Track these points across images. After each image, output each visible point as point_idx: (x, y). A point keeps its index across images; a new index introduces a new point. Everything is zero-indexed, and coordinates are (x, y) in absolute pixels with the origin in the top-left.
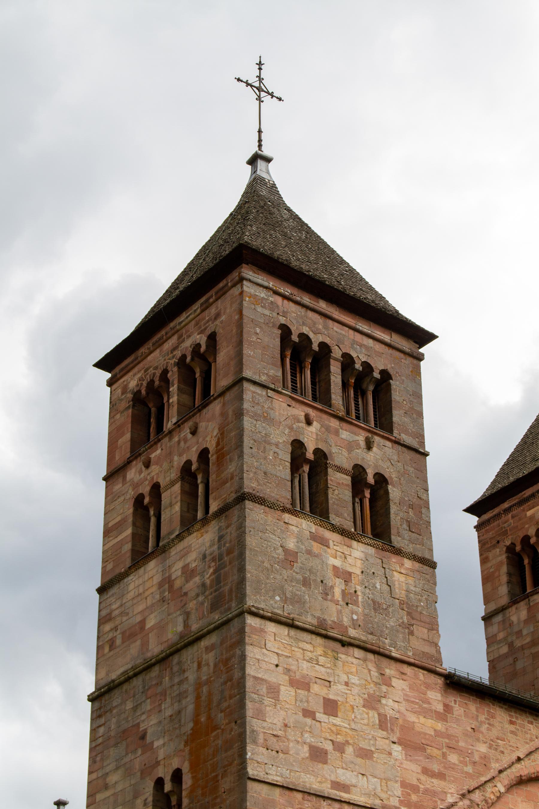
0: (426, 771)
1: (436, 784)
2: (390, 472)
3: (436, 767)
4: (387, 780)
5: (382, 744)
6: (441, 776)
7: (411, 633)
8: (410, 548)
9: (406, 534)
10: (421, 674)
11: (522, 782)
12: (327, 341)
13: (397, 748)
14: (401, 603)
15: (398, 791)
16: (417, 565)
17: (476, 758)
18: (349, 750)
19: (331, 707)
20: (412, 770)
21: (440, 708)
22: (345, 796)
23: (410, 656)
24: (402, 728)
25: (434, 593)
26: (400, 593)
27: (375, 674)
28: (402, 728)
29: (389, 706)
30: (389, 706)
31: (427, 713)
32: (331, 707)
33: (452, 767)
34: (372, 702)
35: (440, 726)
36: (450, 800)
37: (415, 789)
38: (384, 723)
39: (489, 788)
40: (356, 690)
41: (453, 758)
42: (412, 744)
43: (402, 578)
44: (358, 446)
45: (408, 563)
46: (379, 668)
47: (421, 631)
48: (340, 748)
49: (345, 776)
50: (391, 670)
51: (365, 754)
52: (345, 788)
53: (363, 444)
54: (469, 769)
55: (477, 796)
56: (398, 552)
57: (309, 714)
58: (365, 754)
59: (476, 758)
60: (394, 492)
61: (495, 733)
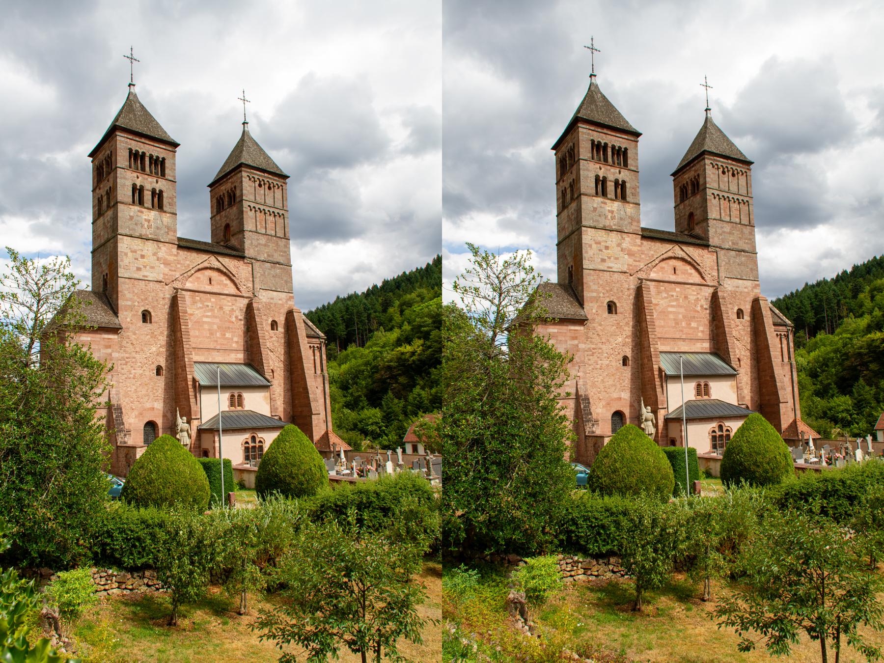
2: (163, 189)
8: (169, 211)
11: (199, 270)
15: (162, 276)
19: (143, 257)
30: (160, 255)
32: (143, 257)
42: (166, 263)
50: (161, 245)
56: (165, 212)
57: (136, 259)
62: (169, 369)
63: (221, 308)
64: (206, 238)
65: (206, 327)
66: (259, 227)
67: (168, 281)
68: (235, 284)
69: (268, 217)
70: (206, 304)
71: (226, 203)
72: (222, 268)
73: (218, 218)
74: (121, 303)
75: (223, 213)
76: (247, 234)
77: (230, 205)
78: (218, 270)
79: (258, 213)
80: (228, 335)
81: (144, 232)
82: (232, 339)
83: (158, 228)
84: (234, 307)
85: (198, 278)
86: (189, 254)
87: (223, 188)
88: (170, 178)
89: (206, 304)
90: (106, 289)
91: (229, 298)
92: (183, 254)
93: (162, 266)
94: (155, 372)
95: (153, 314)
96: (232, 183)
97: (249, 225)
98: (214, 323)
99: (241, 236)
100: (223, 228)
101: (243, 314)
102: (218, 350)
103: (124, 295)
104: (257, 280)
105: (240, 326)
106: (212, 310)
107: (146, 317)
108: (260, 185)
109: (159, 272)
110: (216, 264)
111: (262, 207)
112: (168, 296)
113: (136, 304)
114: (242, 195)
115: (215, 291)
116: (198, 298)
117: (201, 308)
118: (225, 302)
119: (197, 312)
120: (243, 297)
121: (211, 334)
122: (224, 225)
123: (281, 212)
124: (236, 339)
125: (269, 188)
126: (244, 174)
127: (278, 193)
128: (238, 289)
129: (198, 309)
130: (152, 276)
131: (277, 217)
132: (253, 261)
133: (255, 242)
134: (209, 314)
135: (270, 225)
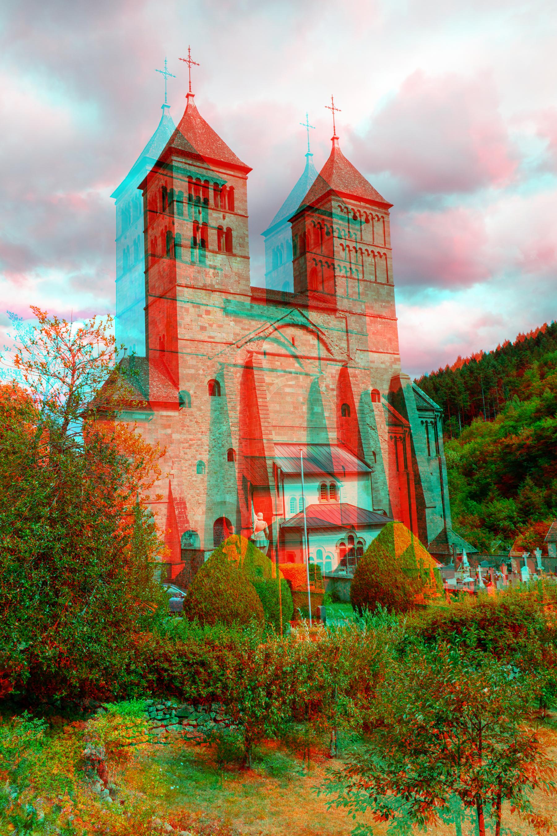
0: (242, 329)
1: (247, 332)
2: (232, 226)
3: (246, 327)
4: (228, 333)
5: (226, 322)
6: (248, 329)
7: (239, 283)
9: (238, 248)
14: (236, 273)
18: (214, 325)
21: (249, 307)
22: (212, 340)
23: (238, 291)
25: (249, 268)
26: (235, 270)
33: (253, 326)
36: (251, 337)
37: (238, 335)
39: (266, 331)
43: (236, 265)
44: (220, 218)
45: (239, 259)
47: (243, 282)
48: (211, 325)
49: (212, 334)
51: (220, 326)
52: (213, 338)
53: (222, 217)
56: (235, 255)
58: (220, 326)
60: (234, 233)
61: (269, 313)
65: (289, 399)
67: (240, 344)
68: (325, 345)
69: (365, 258)
76: (340, 281)
78: (303, 327)
81: (208, 281)
83: (226, 276)
86: (266, 307)
88: (240, 212)
94: (226, 456)
95: (221, 384)
99: (331, 283)
101: (336, 382)
103: (185, 361)
104: (352, 340)
107: (214, 388)
108: (355, 218)
110: (301, 320)
113: (201, 372)
116: (278, 363)
117: (282, 376)
120: (335, 360)
121: (295, 408)
123: (382, 251)
126: (334, 204)
127: (378, 227)
128: (329, 350)
129: (278, 377)
130: (220, 336)
131: (378, 258)
134: (293, 383)
135: (368, 269)
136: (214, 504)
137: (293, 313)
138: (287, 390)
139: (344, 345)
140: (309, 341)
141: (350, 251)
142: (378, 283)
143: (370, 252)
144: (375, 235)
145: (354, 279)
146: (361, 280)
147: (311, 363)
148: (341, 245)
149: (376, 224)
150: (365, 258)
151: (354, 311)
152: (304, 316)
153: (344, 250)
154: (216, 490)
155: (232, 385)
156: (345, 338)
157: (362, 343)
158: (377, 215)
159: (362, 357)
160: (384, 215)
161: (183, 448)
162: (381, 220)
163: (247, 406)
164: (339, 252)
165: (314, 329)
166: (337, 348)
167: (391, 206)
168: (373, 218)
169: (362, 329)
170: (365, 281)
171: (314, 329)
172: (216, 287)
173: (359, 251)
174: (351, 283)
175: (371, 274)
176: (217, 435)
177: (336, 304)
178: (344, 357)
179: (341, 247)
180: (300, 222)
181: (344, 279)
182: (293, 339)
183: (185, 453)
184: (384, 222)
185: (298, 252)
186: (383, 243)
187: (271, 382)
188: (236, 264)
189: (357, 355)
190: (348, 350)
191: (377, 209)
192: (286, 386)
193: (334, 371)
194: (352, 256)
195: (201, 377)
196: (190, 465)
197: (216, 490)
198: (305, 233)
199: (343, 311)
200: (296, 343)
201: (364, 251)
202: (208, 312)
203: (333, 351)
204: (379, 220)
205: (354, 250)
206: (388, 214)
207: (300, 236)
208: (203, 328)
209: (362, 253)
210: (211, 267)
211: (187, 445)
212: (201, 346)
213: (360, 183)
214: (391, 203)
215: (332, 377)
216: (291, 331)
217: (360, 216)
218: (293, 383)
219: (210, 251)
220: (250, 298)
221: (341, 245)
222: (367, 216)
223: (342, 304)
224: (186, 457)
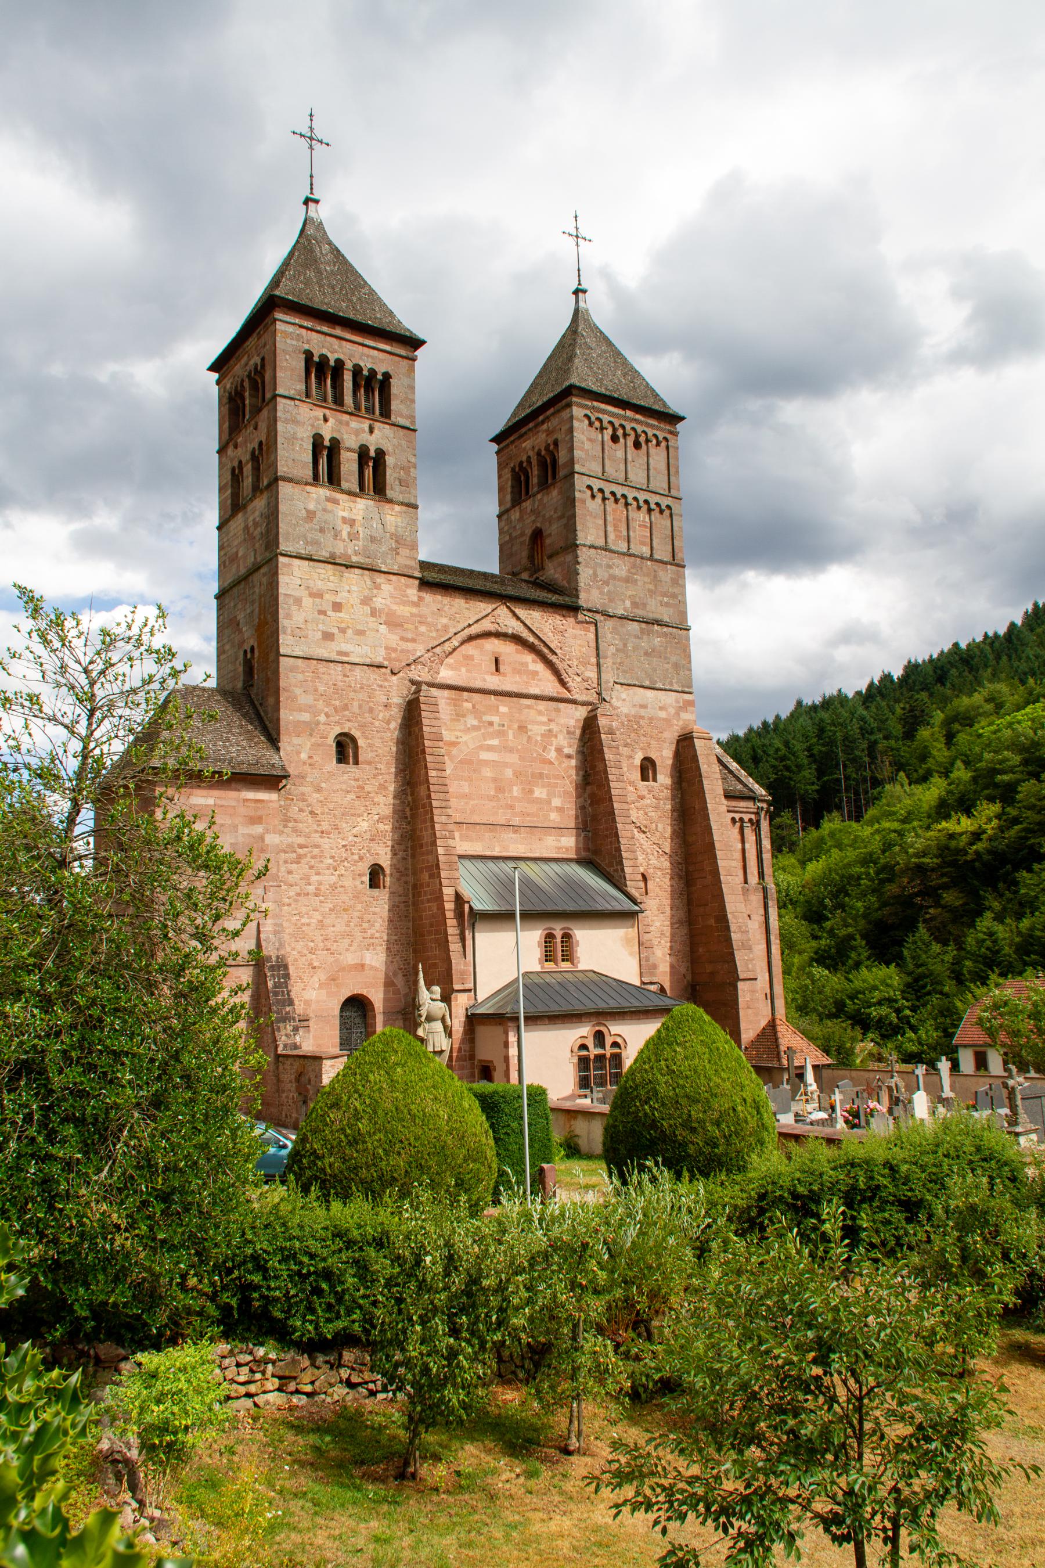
0: (402, 639)
1: (410, 646)
2: (387, 447)
3: (410, 636)
5: (372, 625)
6: (414, 640)
9: (398, 488)
10: (403, 579)
11: (471, 638)
12: (342, 357)
13: (383, 627)
14: (392, 535)
15: (382, 652)
16: (404, 508)
17: (439, 627)
18: (350, 632)
20: (393, 639)
21: (415, 599)
22: (345, 659)
23: (395, 568)
24: (387, 614)
25: (416, 525)
26: (391, 528)
27: (369, 583)
28: (387, 614)
29: (379, 602)
30: (379, 602)
31: (404, 603)
33: (422, 634)
34: (366, 601)
35: (414, 610)
37: (395, 650)
38: (373, 613)
39: (447, 644)
40: (355, 595)
41: (423, 629)
42: (393, 623)
43: (393, 518)
45: (397, 508)
46: (372, 579)
48: (343, 631)
49: (345, 647)
50: (380, 579)
51: (361, 633)
52: (346, 654)
53: (367, 429)
54: (434, 634)
55: (438, 650)
56: (390, 501)
58: (361, 633)
59: (439, 627)
60: (390, 460)
61: (454, 610)
62: (400, 872)
63: (522, 728)
64: (488, 561)
65: (487, 772)
66: (612, 536)
67: (396, 666)
69: (633, 514)
70: (487, 718)
71: (535, 480)
72: (525, 634)
73: (515, 515)
74: (287, 716)
75: (527, 505)
76: (583, 554)
77: (545, 485)
78: (516, 639)
79: (610, 504)
80: (539, 793)
81: (339, 548)
82: (549, 802)
83: (373, 539)
84: (552, 726)
85: (470, 658)
86: (446, 600)
87: (527, 444)
88: (402, 421)
89: (487, 718)
90: (251, 683)
91: (542, 705)
92: (433, 600)
93: (383, 629)
94: (366, 879)
96: (549, 433)
97: (588, 532)
98: (506, 765)
99: (569, 558)
100: (527, 539)
101: (575, 743)
102: (516, 828)
103: (294, 698)
104: (607, 664)
105: (567, 772)
106: (501, 734)
107: (345, 749)
108: (615, 439)
109: (376, 643)
110: (511, 625)
111: (619, 491)
112: (398, 700)
113: (322, 718)
114: (572, 462)
115: (508, 687)
116: (468, 705)
117: (475, 728)
118: (532, 712)
119: (465, 738)
120: (574, 702)
121: (500, 789)
122: (529, 532)
123: (664, 502)
124: (558, 801)
125: (637, 445)
126: (577, 412)
127: (658, 457)
128: (563, 683)
129: (467, 730)
130: (358, 652)
131: (656, 515)
132: (598, 617)
133: (602, 574)
134: (495, 742)
135: (639, 533)
136: (343, 969)
137: (498, 611)
138: (485, 756)
139: (593, 675)
140: (526, 664)
141: (604, 499)
142: (656, 561)
143: (641, 503)
144: (652, 471)
145: (611, 551)
146: (624, 554)
147: (529, 707)
148: (589, 487)
149: (653, 451)
150: (633, 514)
151: (611, 611)
152: (518, 618)
153: (593, 497)
154: (347, 941)
155: (380, 745)
156: (594, 660)
157: (624, 671)
158: (655, 435)
159: (624, 696)
160: (669, 436)
161: (286, 862)
162: (663, 444)
163: (408, 783)
164: (584, 502)
165: (537, 642)
166: (579, 679)
167: (682, 419)
168: (647, 441)
169: (625, 645)
170: (631, 555)
171: (537, 642)
172: (354, 559)
173: (622, 501)
174: (603, 558)
175: (643, 543)
176: (351, 838)
177: (577, 597)
178: (592, 697)
179: (589, 493)
180: (512, 442)
181: (593, 551)
182: (497, 661)
183: (290, 872)
184: (667, 448)
185: (509, 497)
186: (666, 486)
187: (453, 739)
188: (393, 517)
189: (614, 694)
190: (599, 684)
191: (656, 423)
192: (481, 747)
193: (572, 723)
194: (608, 508)
195: (322, 727)
196: (299, 895)
197: (347, 941)
198: (521, 463)
199: (589, 610)
200: (502, 667)
201: (630, 500)
202: (337, 607)
203: (570, 684)
204: (658, 444)
205: (612, 499)
206: (675, 434)
207: (513, 470)
208: (328, 636)
209: (627, 504)
210: (344, 520)
211: (294, 855)
212: (322, 670)
213: (625, 375)
214: (682, 414)
215: (569, 733)
216: (494, 645)
217: (625, 435)
218: (495, 742)
219: (343, 492)
220: (417, 582)
221: (589, 487)
222: (637, 436)
223: (589, 596)
224: (291, 878)
